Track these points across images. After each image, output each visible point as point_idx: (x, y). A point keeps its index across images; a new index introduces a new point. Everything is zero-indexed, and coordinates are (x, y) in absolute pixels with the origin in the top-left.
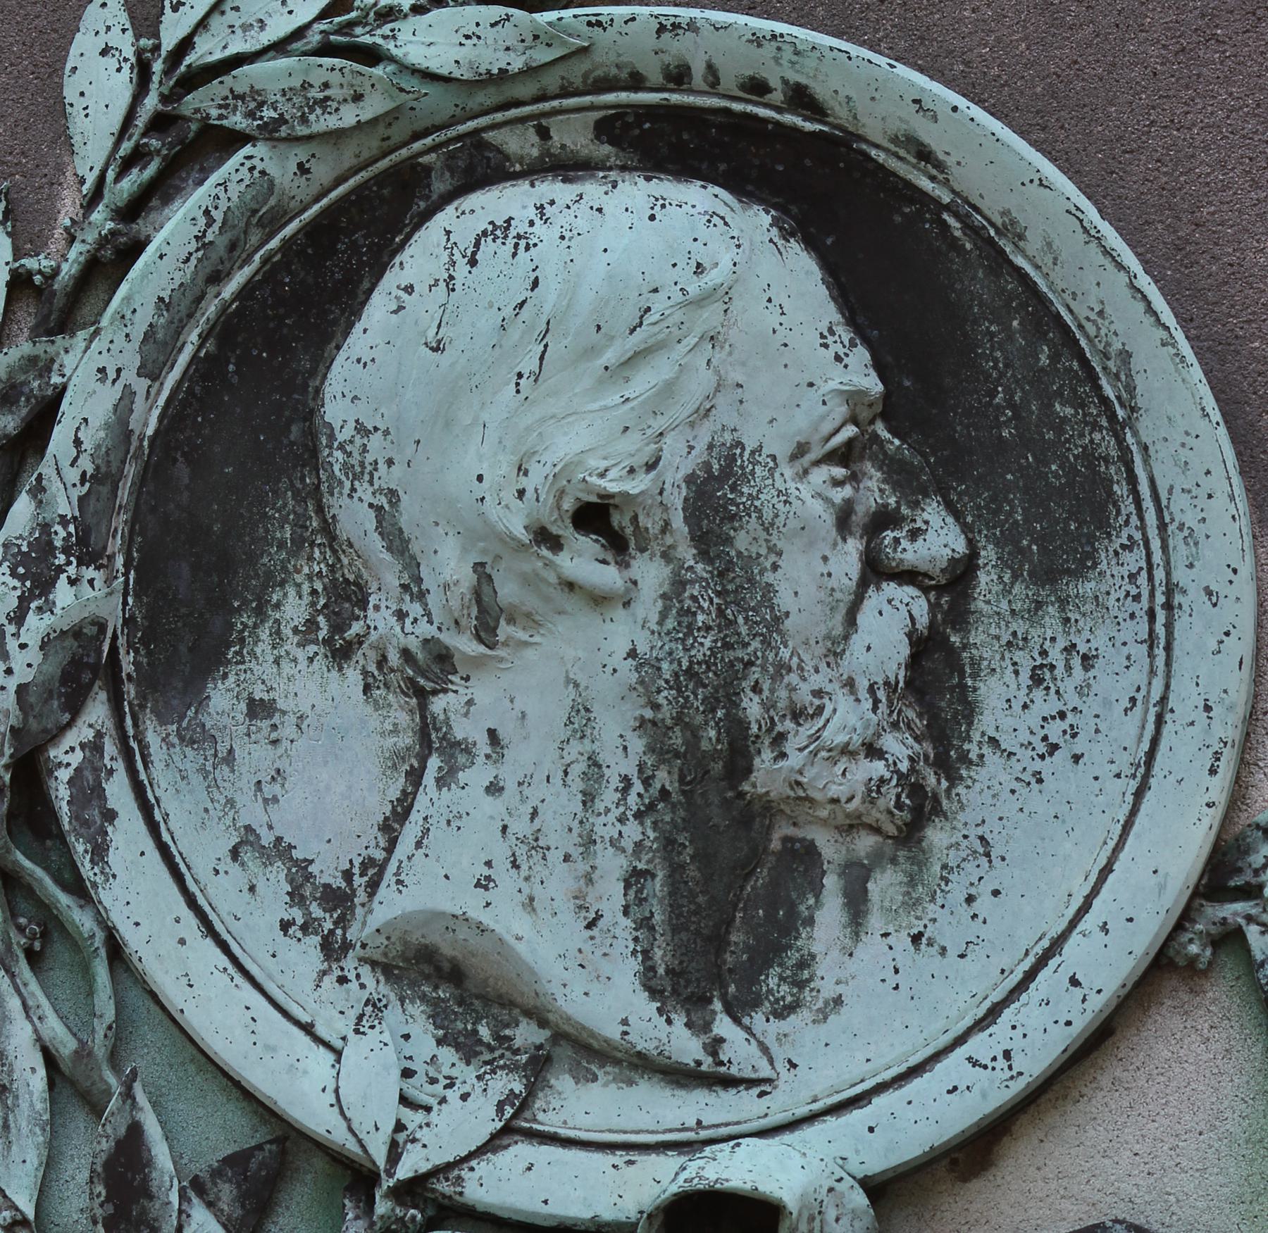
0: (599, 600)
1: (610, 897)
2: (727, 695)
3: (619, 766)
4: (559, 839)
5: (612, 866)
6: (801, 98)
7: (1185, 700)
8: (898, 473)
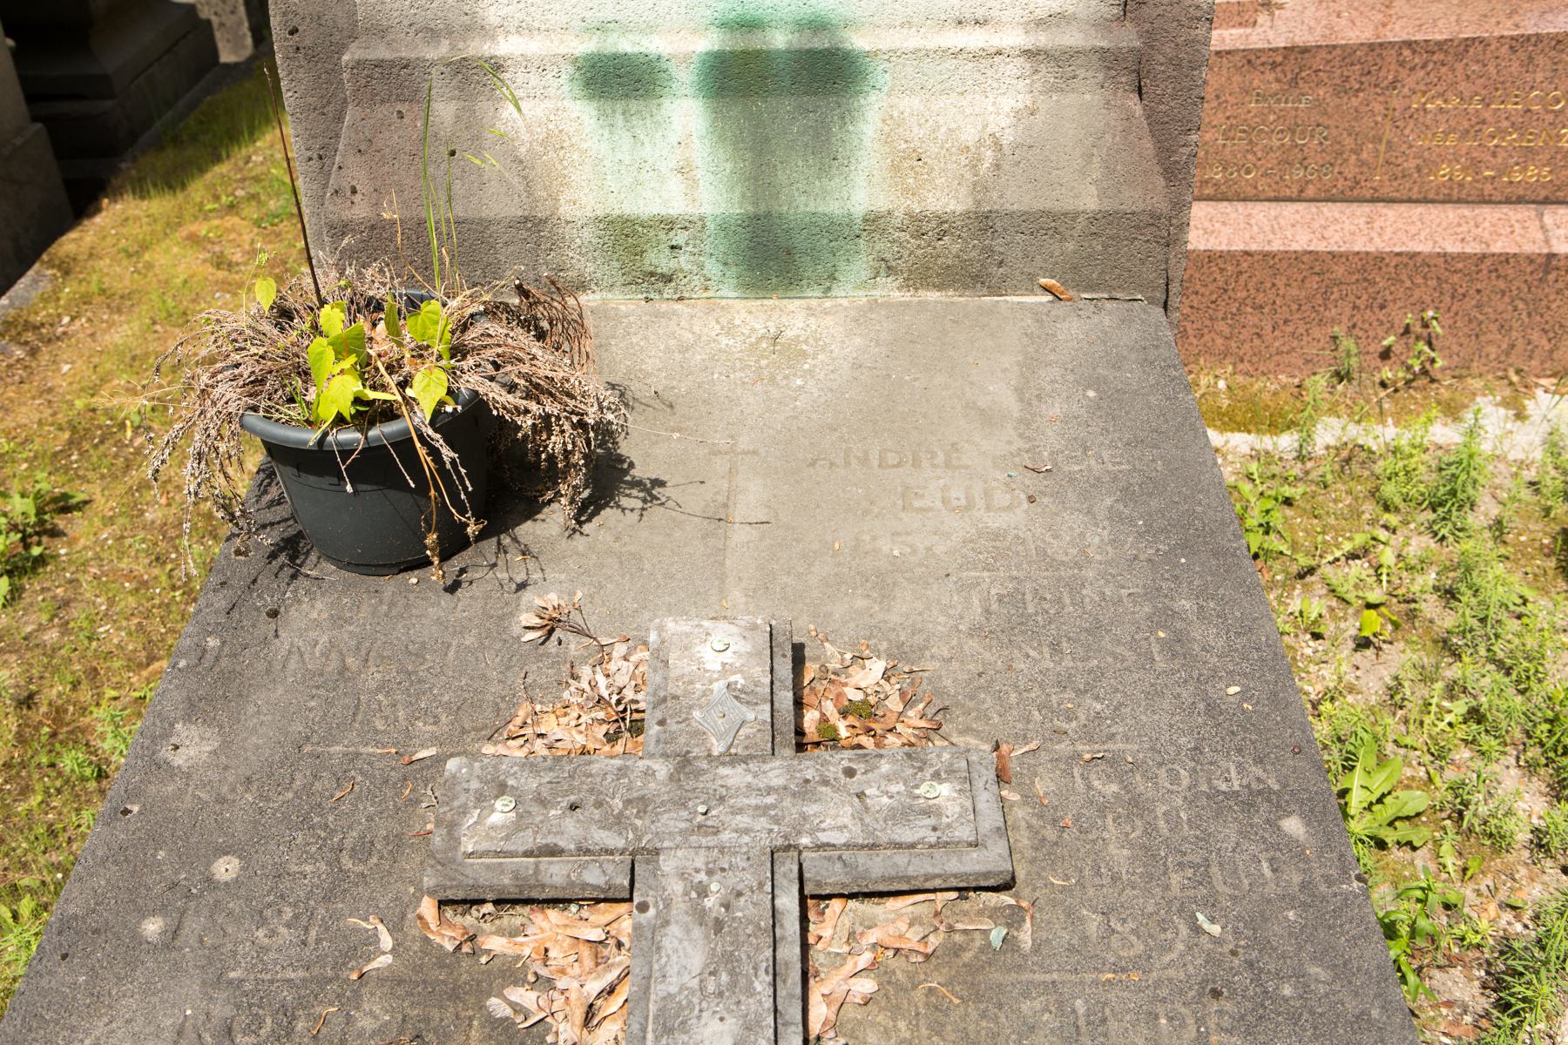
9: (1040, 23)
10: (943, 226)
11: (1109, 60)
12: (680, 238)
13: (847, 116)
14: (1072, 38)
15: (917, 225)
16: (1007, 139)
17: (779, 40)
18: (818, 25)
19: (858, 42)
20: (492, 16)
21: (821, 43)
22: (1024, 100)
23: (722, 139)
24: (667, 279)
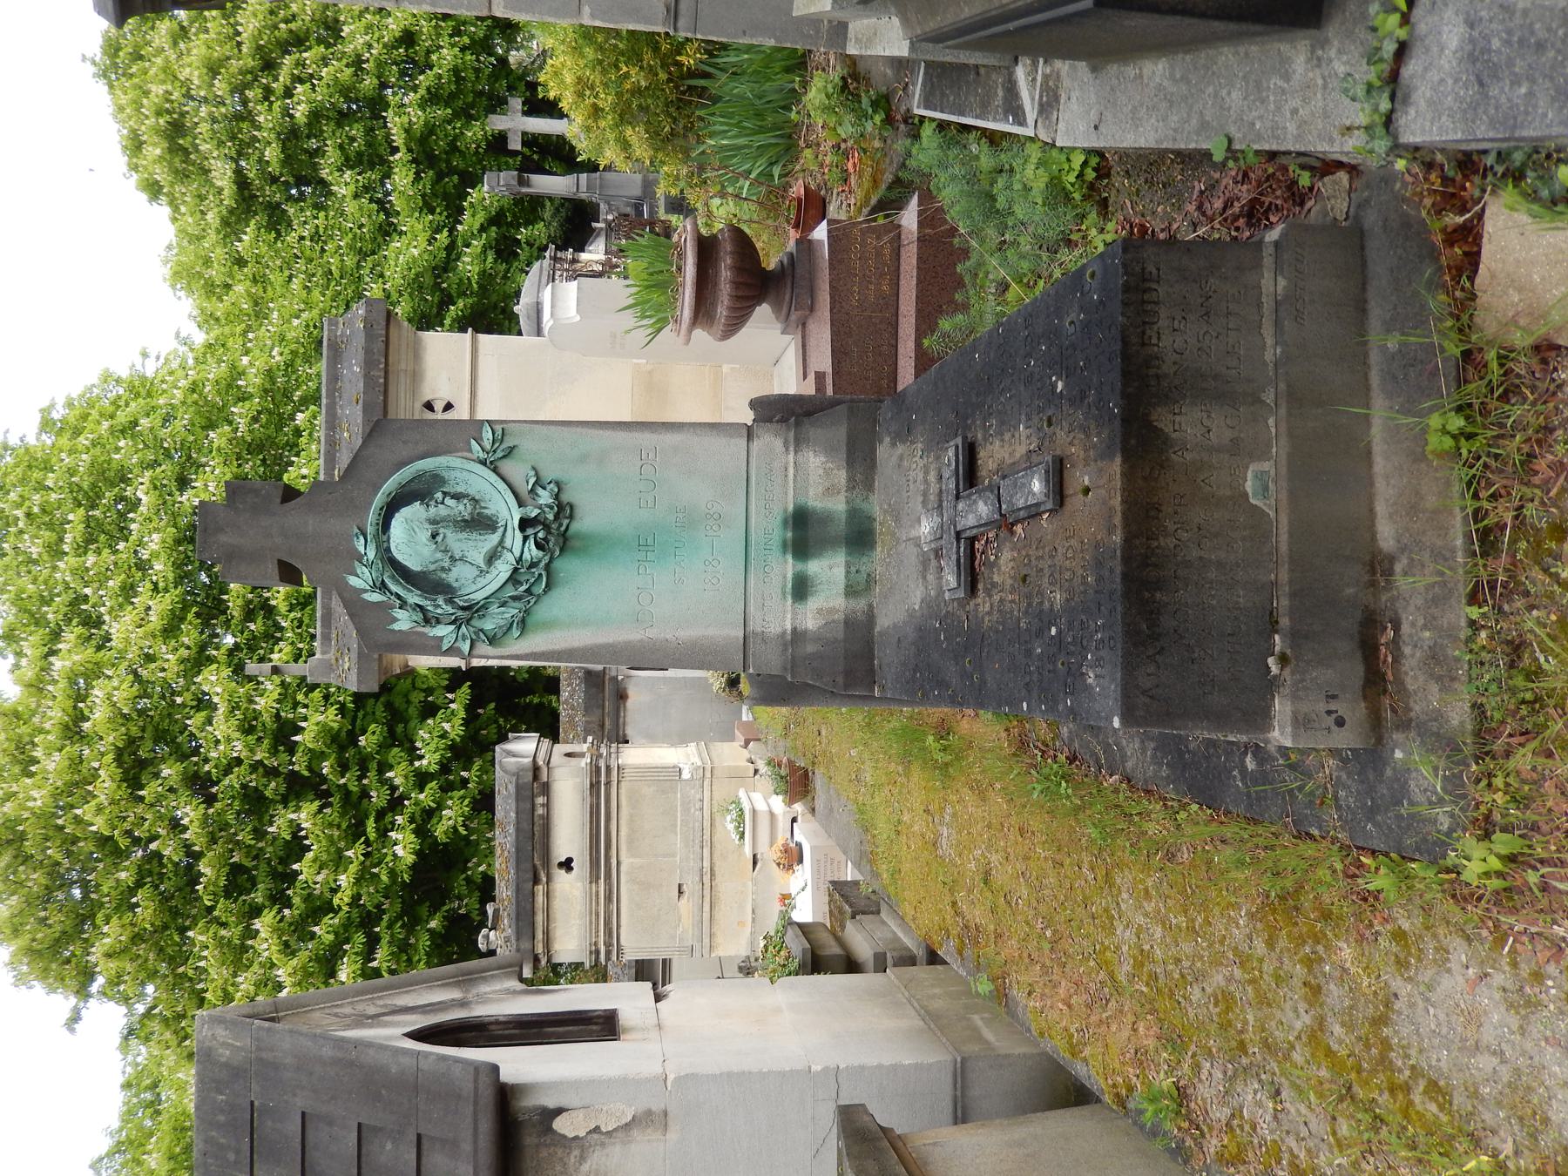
9: (787, 450)
10: (851, 479)
11: (798, 424)
12: (853, 569)
13: (814, 512)
14: (791, 439)
15: (851, 488)
16: (823, 459)
17: (790, 534)
18: (785, 522)
19: (791, 508)
20: (779, 630)
22: (811, 454)
23: (821, 554)
24: (869, 575)
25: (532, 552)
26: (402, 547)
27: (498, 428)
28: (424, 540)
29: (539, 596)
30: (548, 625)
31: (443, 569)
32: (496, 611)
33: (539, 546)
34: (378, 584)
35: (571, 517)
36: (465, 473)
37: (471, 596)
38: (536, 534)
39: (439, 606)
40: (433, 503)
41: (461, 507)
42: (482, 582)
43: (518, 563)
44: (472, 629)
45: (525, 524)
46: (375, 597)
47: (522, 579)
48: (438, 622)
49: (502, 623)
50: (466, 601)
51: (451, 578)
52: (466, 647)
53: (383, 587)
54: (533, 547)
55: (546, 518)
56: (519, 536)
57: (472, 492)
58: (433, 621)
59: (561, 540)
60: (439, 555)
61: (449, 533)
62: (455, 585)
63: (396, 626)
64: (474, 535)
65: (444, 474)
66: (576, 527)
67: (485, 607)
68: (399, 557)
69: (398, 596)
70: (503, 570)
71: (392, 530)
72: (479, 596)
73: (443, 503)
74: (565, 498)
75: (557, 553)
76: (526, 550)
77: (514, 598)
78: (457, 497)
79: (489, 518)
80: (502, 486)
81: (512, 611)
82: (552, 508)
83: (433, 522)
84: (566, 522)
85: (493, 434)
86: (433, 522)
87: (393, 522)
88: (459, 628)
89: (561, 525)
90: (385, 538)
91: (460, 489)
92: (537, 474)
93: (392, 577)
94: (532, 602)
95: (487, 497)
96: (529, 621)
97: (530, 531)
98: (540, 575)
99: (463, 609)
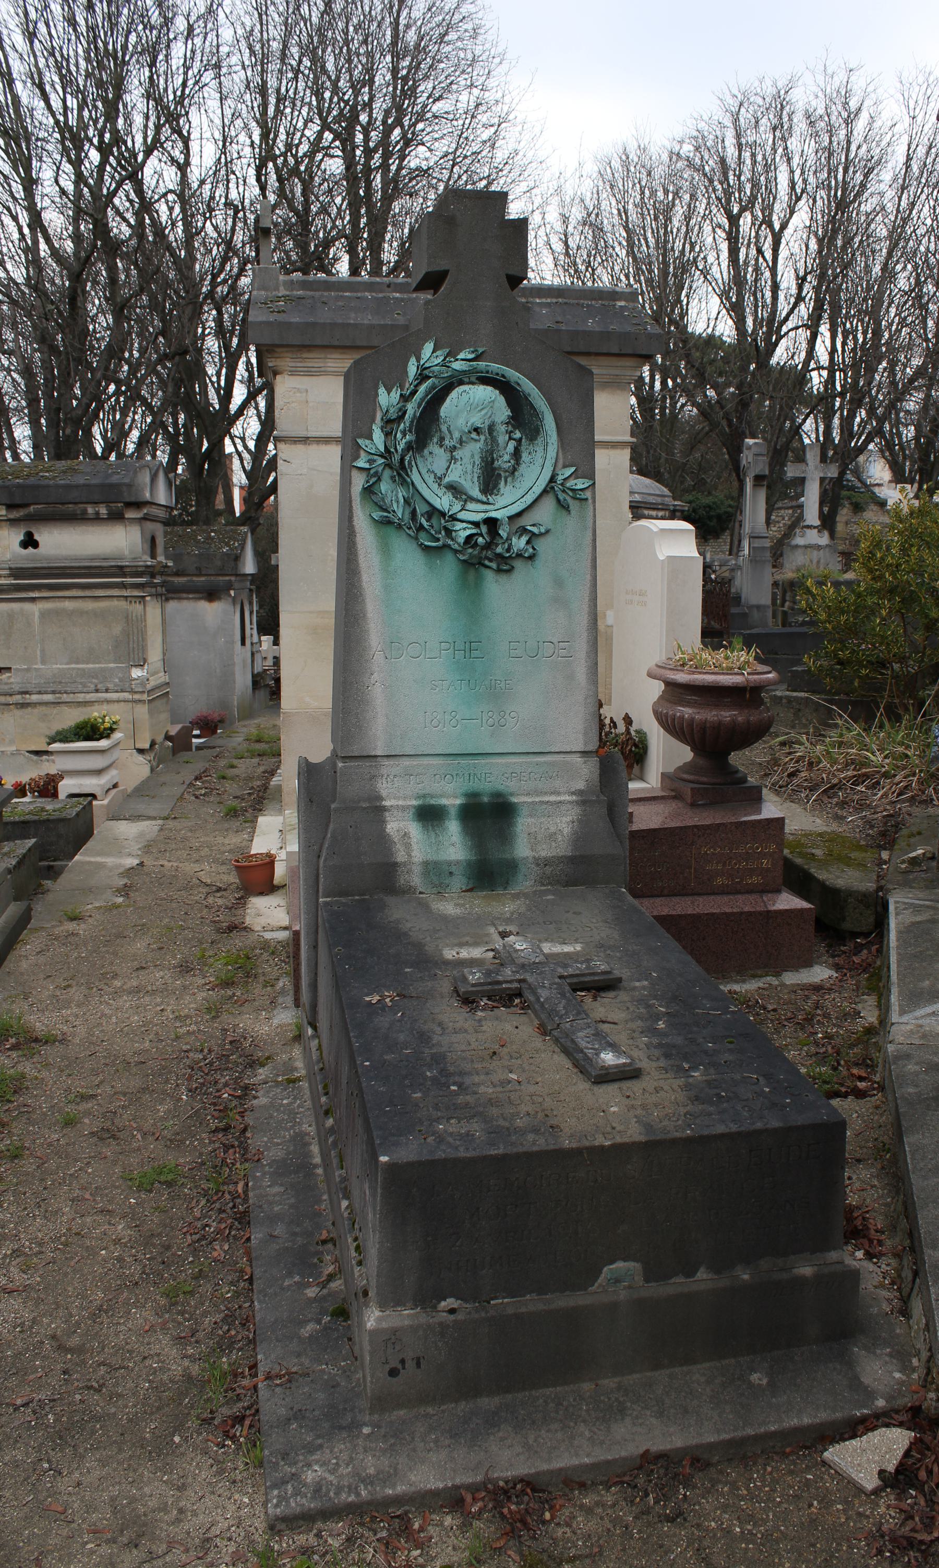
0: (476, 440)
1: (476, 479)
2: (492, 454)
3: (477, 462)
4: (469, 471)
5: (476, 475)
6: (503, 376)
7: (549, 457)
8: (513, 426)
17: (486, 799)
18: (498, 795)
19: (514, 800)
21: (501, 800)
25: (462, 532)
26: (465, 397)
27: (588, 494)
28: (472, 420)
29: (416, 539)
30: (385, 550)
31: (442, 439)
32: (400, 495)
33: (469, 538)
34: (426, 372)
35: (499, 571)
36: (541, 461)
37: (414, 469)
38: (481, 535)
39: (404, 435)
40: (510, 428)
41: (506, 457)
42: (430, 479)
43: (451, 516)
44: (380, 469)
45: (492, 523)
46: (412, 369)
47: (434, 521)
48: (387, 435)
49: (388, 501)
50: (410, 463)
51: (433, 447)
52: (361, 463)
53: (422, 377)
54: (468, 532)
55: (497, 545)
56: (478, 517)
57: (522, 468)
58: (388, 429)
59: (474, 561)
60: (456, 435)
61: (478, 446)
62: (426, 452)
63: (382, 391)
64: (477, 471)
65: (540, 440)
66: (489, 576)
67: (404, 483)
68: (454, 394)
69: (414, 393)
70: (443, 501)
71: (482, 387)
72: (415, 477)
73: (510, 438)
74: (518, 564)
75: (462, 557)
76: (465, 525)
77: (414, 513)
78: (517, 454)
79: (496, 486)
80: (529, 499)
81: (399, 510)
82: (508, 550)
83: (491, 428)
84: (494, 565)
85: (581, 490)
86: (491, 428)
87: (490, 388)
88: (382, 456)
89: (491, 560)
90: (473, 379)
91: (525, 456)
92: (541, 534)
93: (433, 387)
94: (411, 532)
95: (517, 485)
96: (391, 530)
97: (484, 529)
98: (438, 540)
99: (402, 460)
